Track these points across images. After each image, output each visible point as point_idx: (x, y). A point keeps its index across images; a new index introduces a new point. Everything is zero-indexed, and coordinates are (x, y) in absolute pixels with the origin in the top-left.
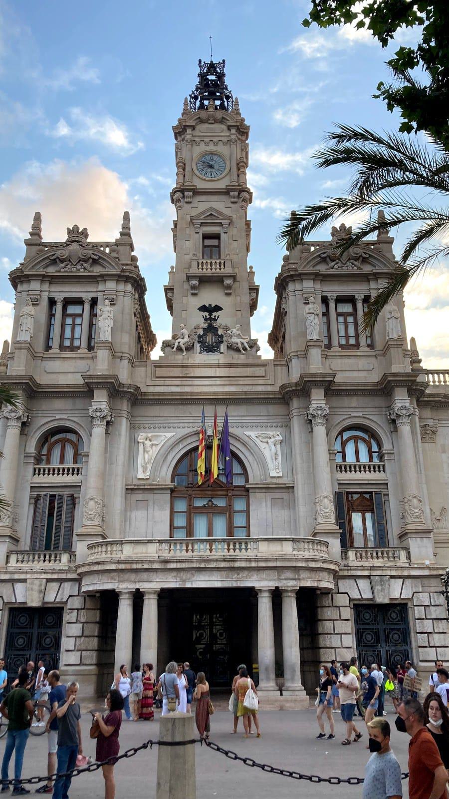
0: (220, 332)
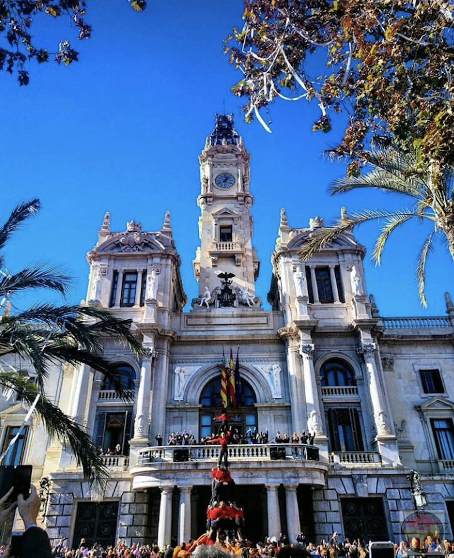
0: (233, 292)
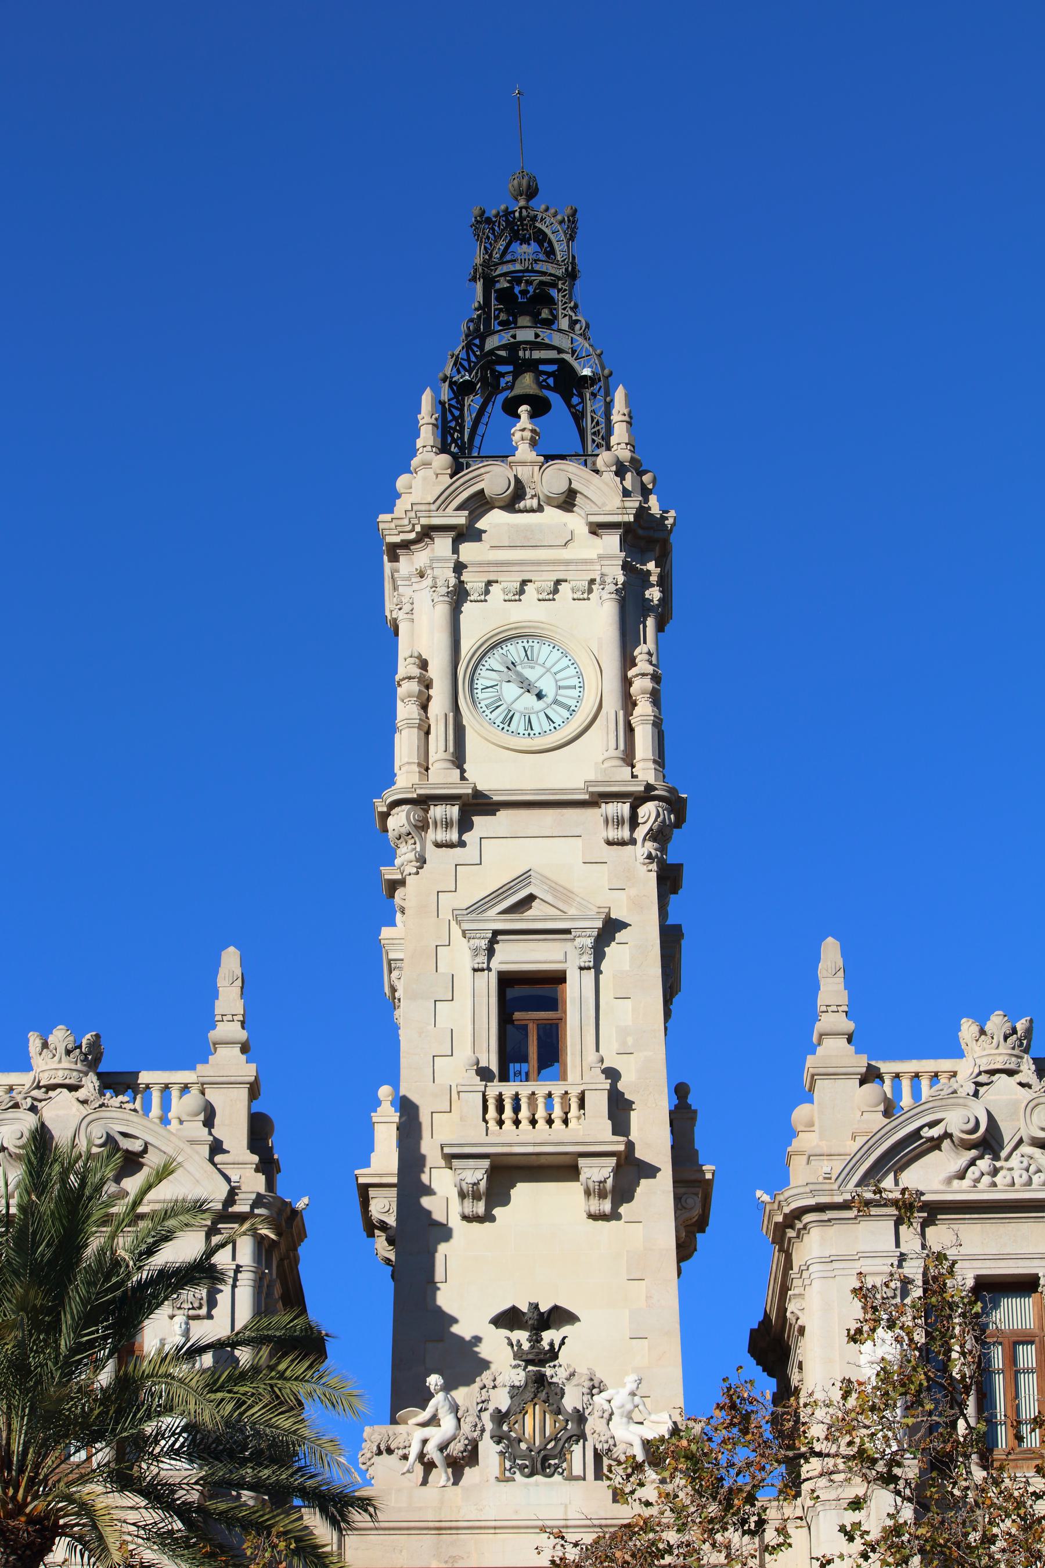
0: (571, 1401)
